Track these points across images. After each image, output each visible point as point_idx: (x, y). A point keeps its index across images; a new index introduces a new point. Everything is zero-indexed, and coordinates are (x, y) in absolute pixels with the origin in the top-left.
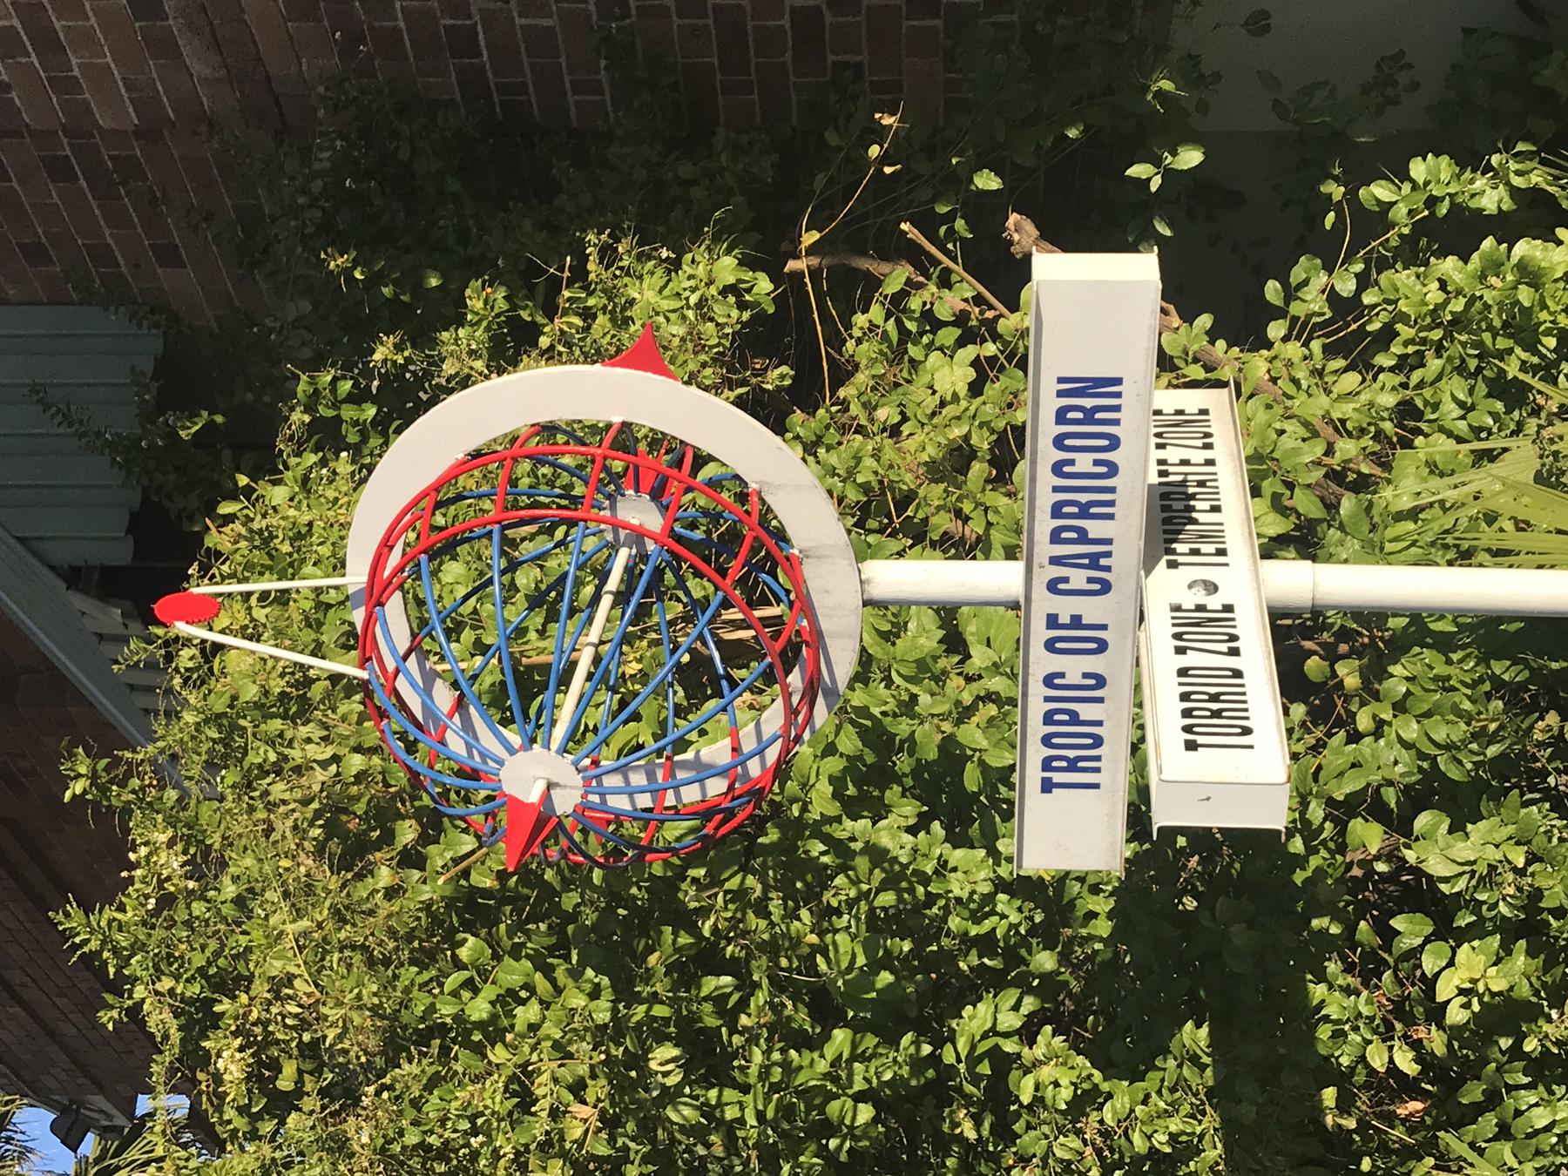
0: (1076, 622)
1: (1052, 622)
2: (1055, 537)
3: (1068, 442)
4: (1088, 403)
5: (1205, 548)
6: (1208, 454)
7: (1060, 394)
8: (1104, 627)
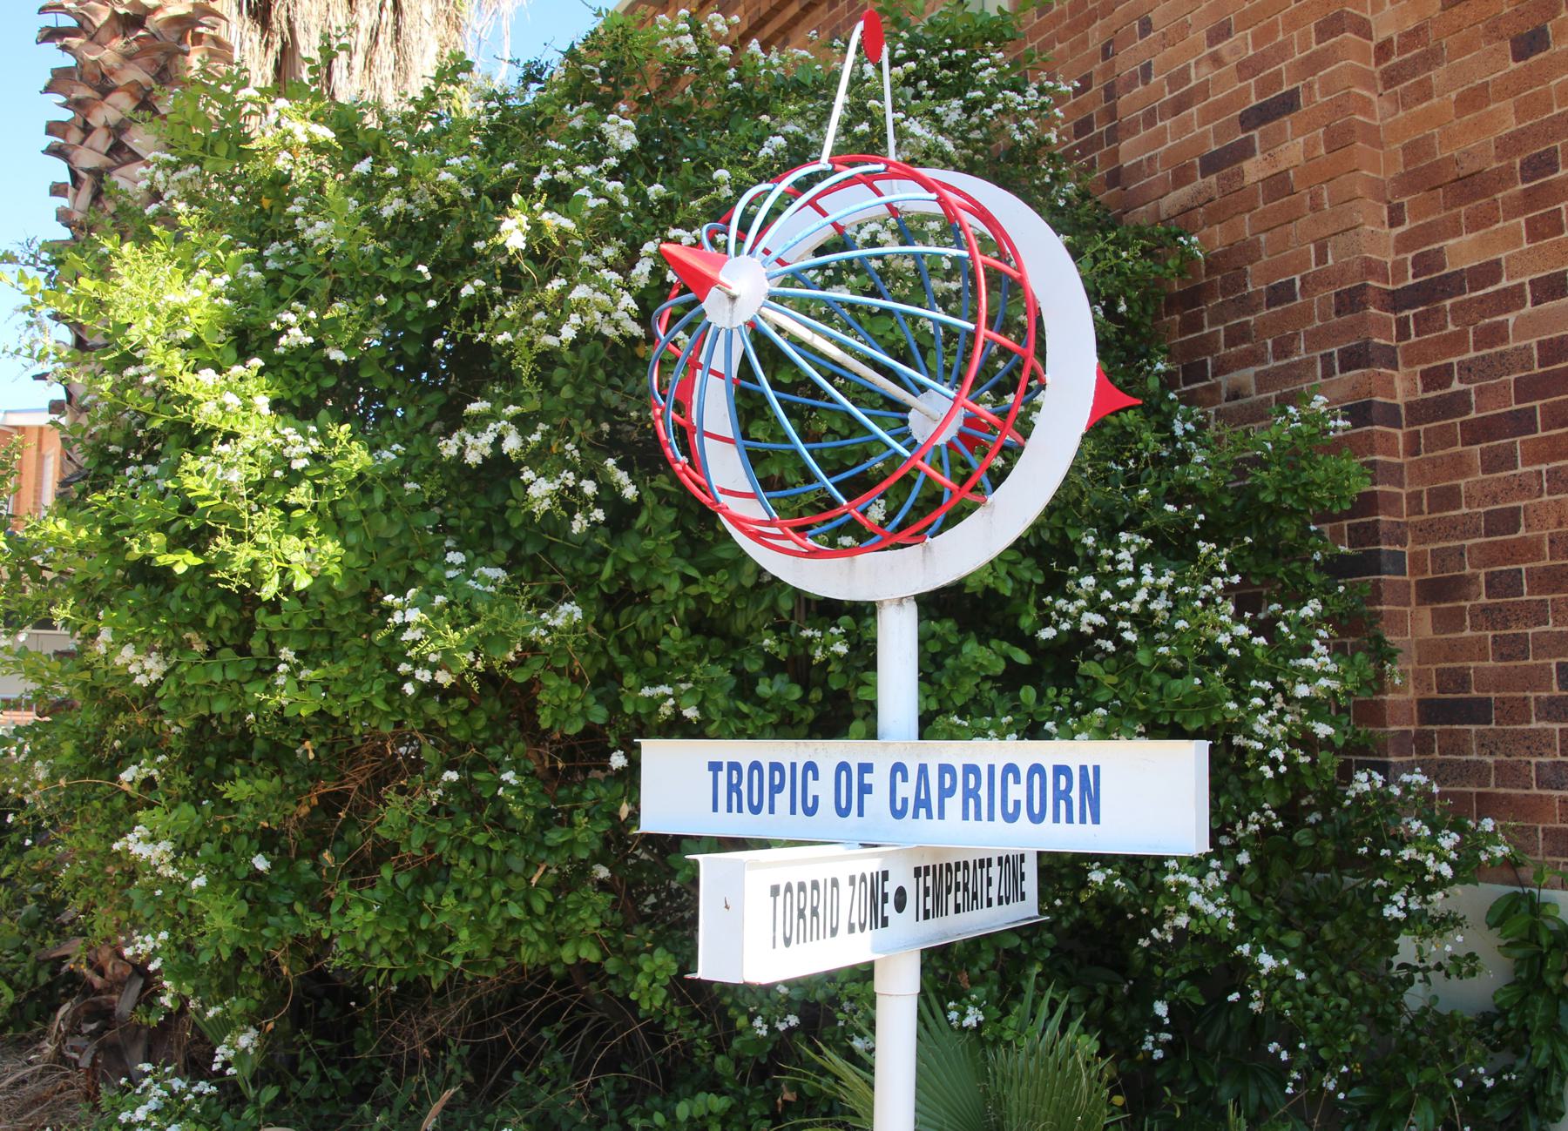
0: (865, 789)
1: (866, 768)
2: (945, 769)
3: (1037, 777)
4: (1075, 794)
5: (929, 899)
6: (995, 901)
7: (1083, 768)
8: (861, 814)
